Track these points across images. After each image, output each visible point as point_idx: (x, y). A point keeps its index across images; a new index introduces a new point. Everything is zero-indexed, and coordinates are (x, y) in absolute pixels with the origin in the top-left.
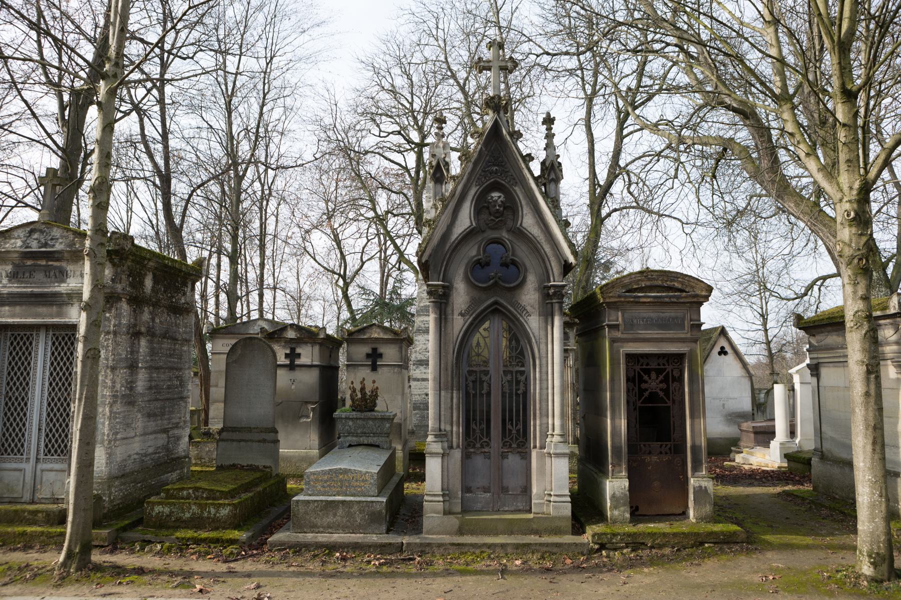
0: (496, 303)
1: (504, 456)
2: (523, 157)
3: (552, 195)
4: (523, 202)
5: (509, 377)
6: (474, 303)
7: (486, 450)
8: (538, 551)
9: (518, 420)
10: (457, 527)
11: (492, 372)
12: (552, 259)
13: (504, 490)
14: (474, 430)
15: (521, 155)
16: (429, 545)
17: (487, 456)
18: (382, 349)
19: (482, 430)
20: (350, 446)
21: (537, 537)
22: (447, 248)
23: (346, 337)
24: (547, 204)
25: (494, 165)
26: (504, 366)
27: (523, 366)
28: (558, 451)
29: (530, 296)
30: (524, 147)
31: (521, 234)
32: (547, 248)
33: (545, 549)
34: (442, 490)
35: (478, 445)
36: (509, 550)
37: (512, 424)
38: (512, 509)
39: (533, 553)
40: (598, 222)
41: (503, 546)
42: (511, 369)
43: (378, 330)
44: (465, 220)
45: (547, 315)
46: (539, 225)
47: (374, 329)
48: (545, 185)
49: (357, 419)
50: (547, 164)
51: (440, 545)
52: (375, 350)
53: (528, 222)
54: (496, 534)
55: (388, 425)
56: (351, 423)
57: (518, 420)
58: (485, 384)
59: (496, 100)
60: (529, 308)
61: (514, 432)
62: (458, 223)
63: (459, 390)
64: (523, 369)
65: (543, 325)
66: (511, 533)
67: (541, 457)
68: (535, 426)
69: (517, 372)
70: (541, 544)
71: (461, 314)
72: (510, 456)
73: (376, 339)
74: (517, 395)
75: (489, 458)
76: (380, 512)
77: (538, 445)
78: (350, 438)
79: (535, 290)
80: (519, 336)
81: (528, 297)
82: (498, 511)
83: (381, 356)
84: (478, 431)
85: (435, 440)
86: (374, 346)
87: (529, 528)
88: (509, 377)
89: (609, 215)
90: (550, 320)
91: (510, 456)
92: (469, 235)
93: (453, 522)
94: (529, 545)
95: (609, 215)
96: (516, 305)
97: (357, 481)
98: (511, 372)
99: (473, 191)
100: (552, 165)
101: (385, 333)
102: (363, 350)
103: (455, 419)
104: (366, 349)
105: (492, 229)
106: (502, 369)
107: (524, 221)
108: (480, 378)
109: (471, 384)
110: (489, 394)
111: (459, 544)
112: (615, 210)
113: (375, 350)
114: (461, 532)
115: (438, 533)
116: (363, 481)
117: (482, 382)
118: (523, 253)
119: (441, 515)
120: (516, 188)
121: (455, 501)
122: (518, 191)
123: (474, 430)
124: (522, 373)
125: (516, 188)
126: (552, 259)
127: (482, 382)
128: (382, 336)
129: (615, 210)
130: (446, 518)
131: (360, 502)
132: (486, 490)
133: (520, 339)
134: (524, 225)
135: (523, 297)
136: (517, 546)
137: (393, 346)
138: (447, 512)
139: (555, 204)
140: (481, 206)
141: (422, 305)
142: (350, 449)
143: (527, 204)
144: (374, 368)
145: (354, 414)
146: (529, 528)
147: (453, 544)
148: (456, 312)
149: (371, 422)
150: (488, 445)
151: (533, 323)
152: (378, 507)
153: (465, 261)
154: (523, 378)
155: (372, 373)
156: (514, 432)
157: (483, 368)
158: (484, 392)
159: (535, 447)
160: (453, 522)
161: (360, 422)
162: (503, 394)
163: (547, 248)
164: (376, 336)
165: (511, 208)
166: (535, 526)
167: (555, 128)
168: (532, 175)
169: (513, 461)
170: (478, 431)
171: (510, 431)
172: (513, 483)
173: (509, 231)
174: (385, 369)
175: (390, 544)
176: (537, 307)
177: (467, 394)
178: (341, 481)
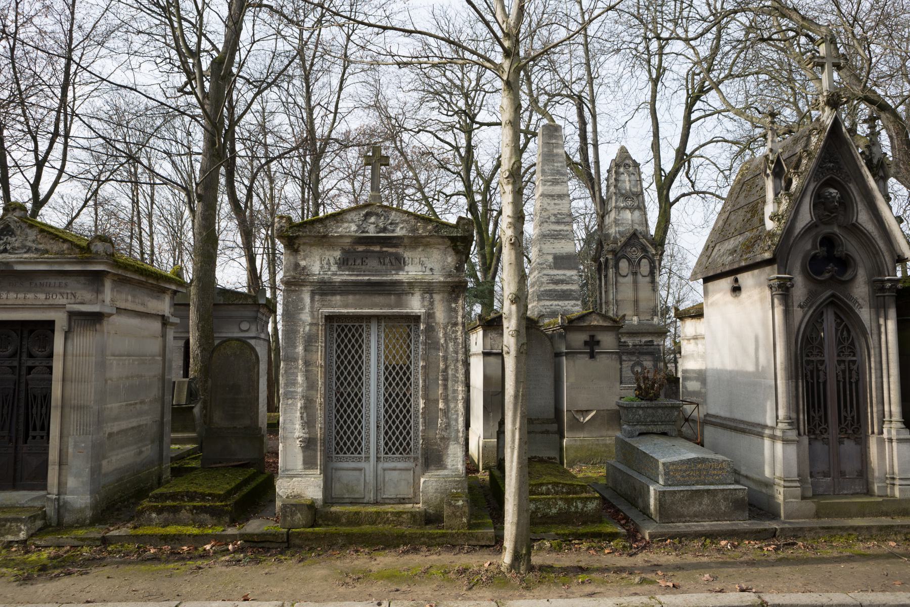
0: (833, 295)
1: (841, 442)
4: (858, 199)
5: (842, 366)
6: (812, 296)
7: (825, 436)
8: (900, 533)
9: (819, 406)
10: (814, 511)
11: (827, 361)
12: (886, 254)
13: (842, 474)
14: (813, 417)
16: (801, 529)
17: (826, 442)
18: (600, 337)
19: (820, 417)
20: (641, 434)
21: (889, 519)
22: (792, 241)
23: (566, 324)
25: (830, 162)
26: (839, 355)
27: (854, 356)
28: (902, 437)
29: (860, 290)
31: (855, 229)
32: (881, 244)
33: (906, 531)
34: (799, 476)
35: (818, 432)
36: (874, 532)
37: (814, 412)
38: (851, 492)
39: (896, 534)
40: (668, 206)
41: (869, 528)
42: (843, 358)
43: (598, 318)
44: (806, 217)
45: (879, 308)
46: (872, 221)
47: (594, 316)
49: (648, 407)
51: (811, 529)
52: (592, 337)
53: (863, 218)
54: (850, 516)
55: (676, 413)
56: (641, 412)
57: (819, 406)
58: (821, 373)
59: (835, 98)
60: (860, 301)
61: (849, 418)
62: (800, 217)
63: (802, 379)
64: (854, 358)
65: (874, 317)
66: (863, 515)
67: (881, 442)
68: (873, 412)
69: (850, 361)
70: (902, 526)
71: (800, 306)
72: (846, 441)
73: (595, 326)
74: (851, 383)
75: (828, 444)
76: (743, 499)
77: (876, 430)
78: (638, 427)
79: (865, 283)
80: (850, 327)
81: (859, 290)
82: (838, 495)
83: (598, 343)
84: (817, 418)
85: (789, 427)
86: (592, 333)
87: (878, 510)
88: (842, 366)
89: (677, 200)
90: (882, 312)
91: (846, 441)
92: (808, 229)
93: (810, 506)
94: (891, 527)
95: (677, 200)
96: (850, 297)
97: (714, 469)
98: (844, 361)
99: (811, 187)
101: (604, 321)
102: (578, 339)
103: (801, 407)
104: (583, 337)
105: (825, 224)
106: (836, 358)
107: (860, 217)
108: (817, 368)
109: (840, 374)
110: (825, 383)
111: (828, 528)
112: (684, 195)
113: (592, 337)
114: (818, 515)
115: (798, 518)
116: (720, 469)
117: (818, 370)
118: (851, 246)
119: (799, 500)
121: (807, 486)
122: (853, 188)
123: (813, 417)
124: (854, 362)
125: (851, 185)
126: (886, 254)
127: (850, 371)
128: (601, 323)
129: (684, 195)
130: (804, 502)
131: (723, 490)
132: (826, 475)
133: (851, 329)
134: (859, 221)
135: (855, 290)
136: (881, 528)
137: (610, 333)
138: (804, 498)
140: (819, 202)
141: (542, 289)
142: (640, 437)
143: (862, 200)
144: (592, 355)
145: (644, 403)
146: (878, 510)
147: (823, 528)
148: (796, 304)
149: (660, 411)
150: (826, 430)
151: (865, 314)
152: (741, 495)
153: (801, 256)
154: (855, 367)
155: (590, 361)
156: (849, 418)
157: (819, 358)
158: (853, 380)
159: (873, 433)
160: (810, 506)
161: (650, 411)
162: (838, 381)
163: (881, 244)
164: (595, 323)
165: (846, 203)
166: (884, 509)
169: (849, 446)
170: (817, 418)
171: (845, 417)
172: (851, 467)
173: (839, 226)
174: (603, 356)
175: (765, 530)
176: (867, 299)
177: (807, 382)
178: (699, 470)
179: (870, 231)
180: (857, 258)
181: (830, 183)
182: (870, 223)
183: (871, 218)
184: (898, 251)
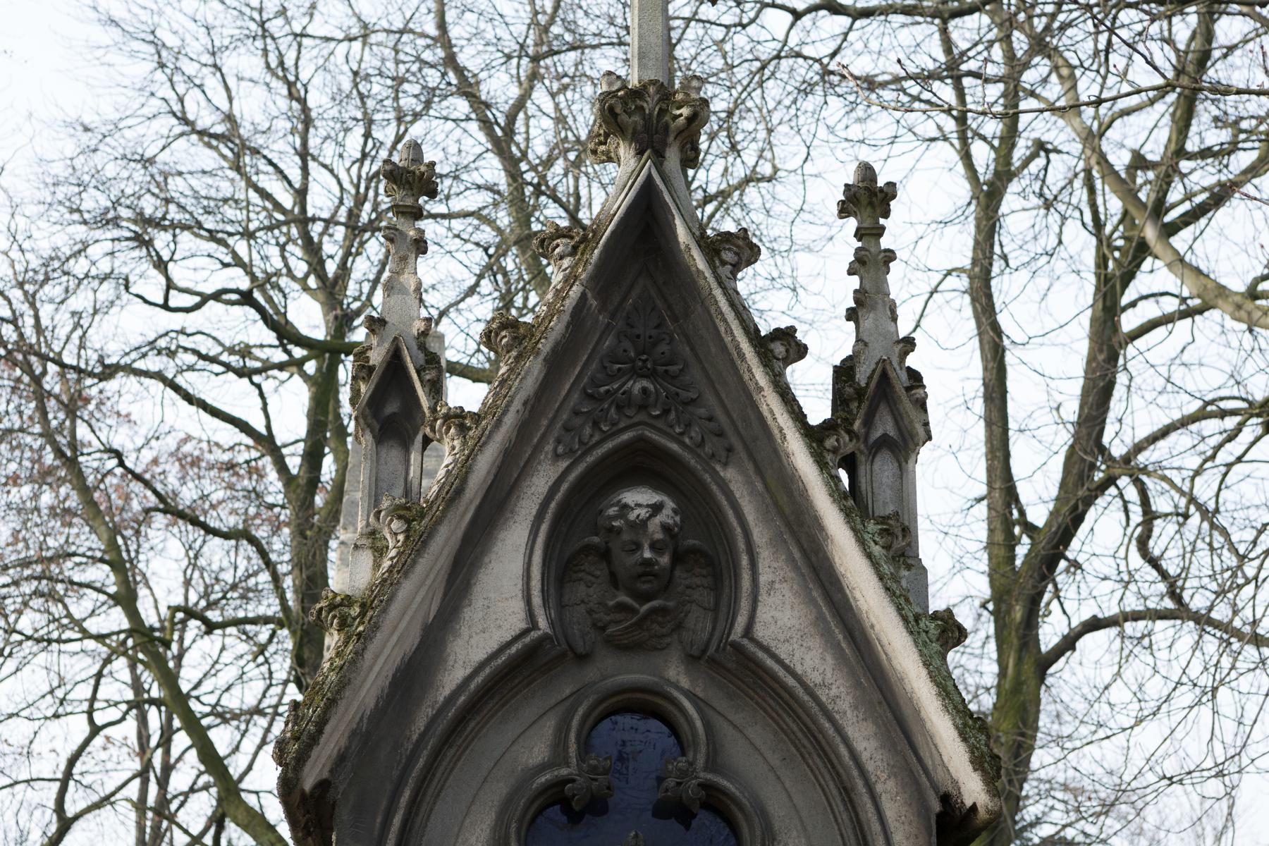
3: (884, 504)
4: (760, 535)
15: (752, 331)
22: (420, 724)
24: (861, 542)
25: (637, 374)
30: (766, 295)
31: (748, 672)
32: (864, 739)
44: (504, 604)
46: (826, 635)
48: (850, 463)
50: (862, 375)
53: (779, 618)
62: (472, 615)
99: (540, 482)
100: (884, 378)
105: (625, 646)
107: (763, 614)
118: (754, 761)
120: (730, 474)
125: (730, 474)
134: (760, 632)
143: (777, 542)
153: (498, 790)
163: (864, 739)
165: (706, 554)
167: (897, 231)
168: (798, 415)
173: (693, 659)
179: (814, 678)
180: (777, 808)
181: (642, 464)
182: (816, 643)
183: (820, 618)
184: (939, 775)
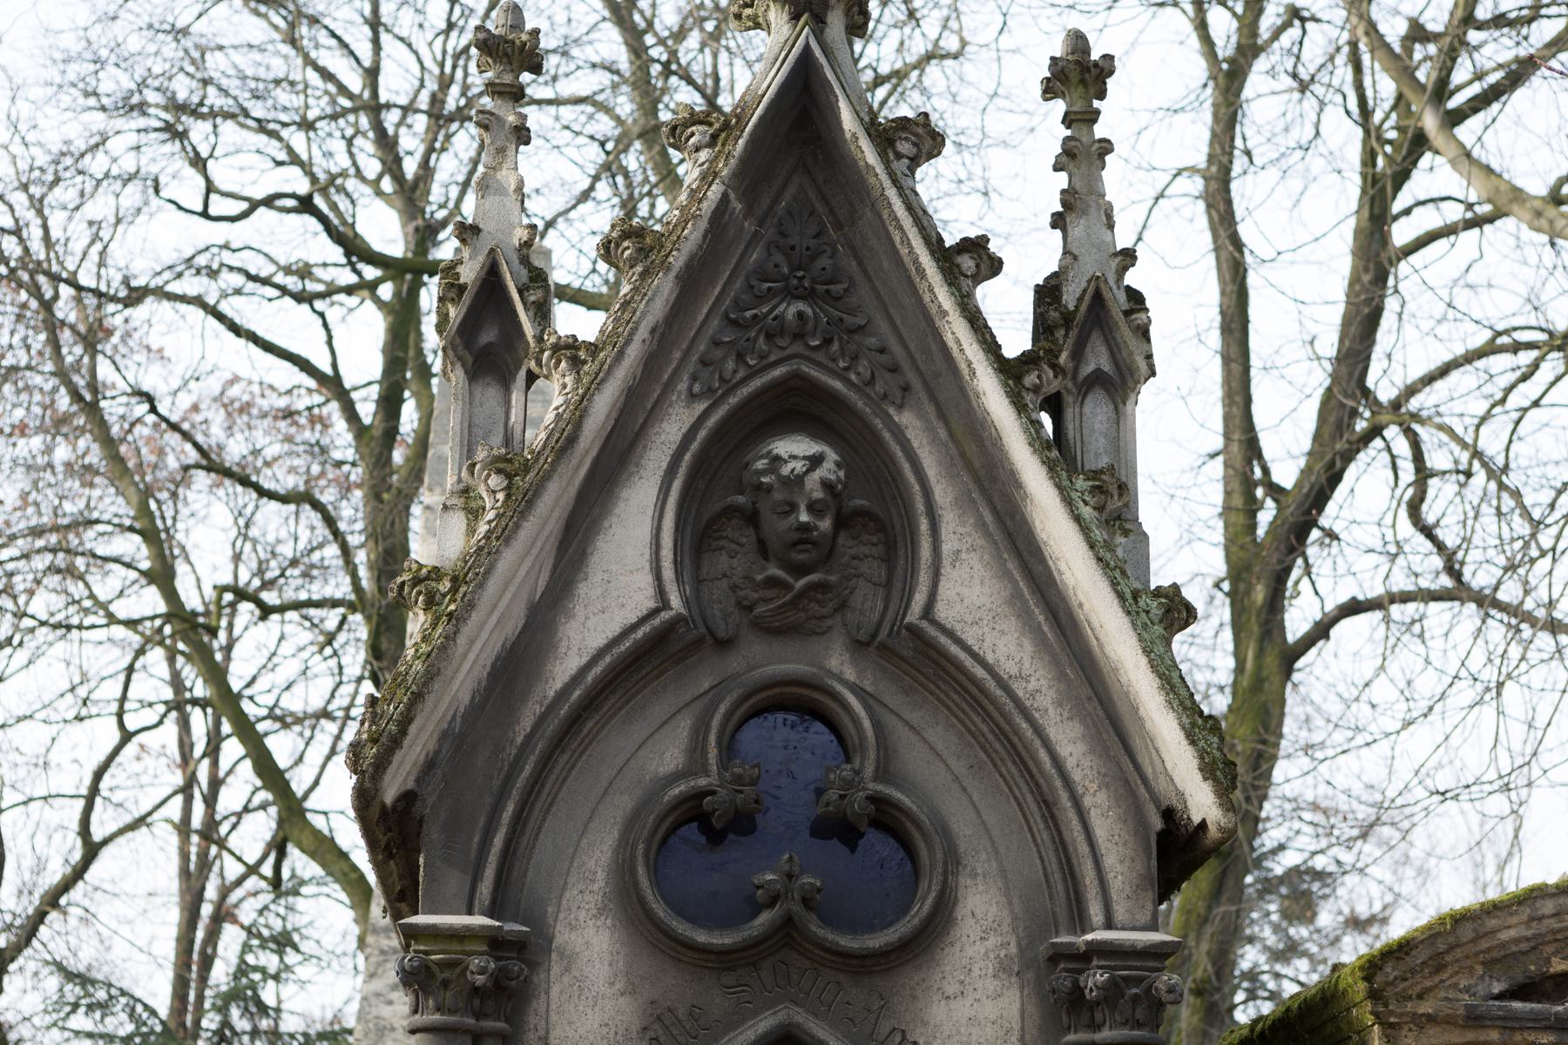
2: (947, 257)
3: (1096, 455)
4: (943, 494)
22: (526, 723)
24: (1068, 502)
25: (792, 294)
30: (951, 197)
31: (927, 661)
32: (1069, 741)
44: (627, 579)
46: (1024, 615)
48: (1054, 405)
50: (1070, 296)
53: (967, 596)
62: (589, 590)
79: (1003, 968)
81: (963, 1009)
92: (646, 658)
100: (1098, 300)
107: (947, 590)
118: (934, 768)
120: (906, 419)
125: (906, 419)
134: (943, 612)
135: (938, 1012)
139: (1109, 504)
140: (718, 505)
143: (964, 502)
153: (621, 804)
163: (1069, 741)
165: (876, 517)
167: (1114, 116)
168: (991, 346)
173: (860, 646)
179: (1008, 668)
180: (963, 826)
181: (797, 406)
182: (1011, 626)
183: (1016, 595)
184: (1161, 786)
